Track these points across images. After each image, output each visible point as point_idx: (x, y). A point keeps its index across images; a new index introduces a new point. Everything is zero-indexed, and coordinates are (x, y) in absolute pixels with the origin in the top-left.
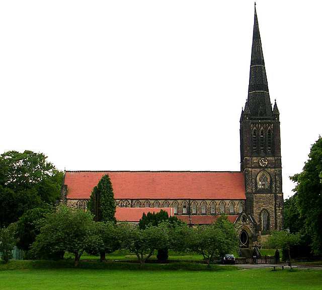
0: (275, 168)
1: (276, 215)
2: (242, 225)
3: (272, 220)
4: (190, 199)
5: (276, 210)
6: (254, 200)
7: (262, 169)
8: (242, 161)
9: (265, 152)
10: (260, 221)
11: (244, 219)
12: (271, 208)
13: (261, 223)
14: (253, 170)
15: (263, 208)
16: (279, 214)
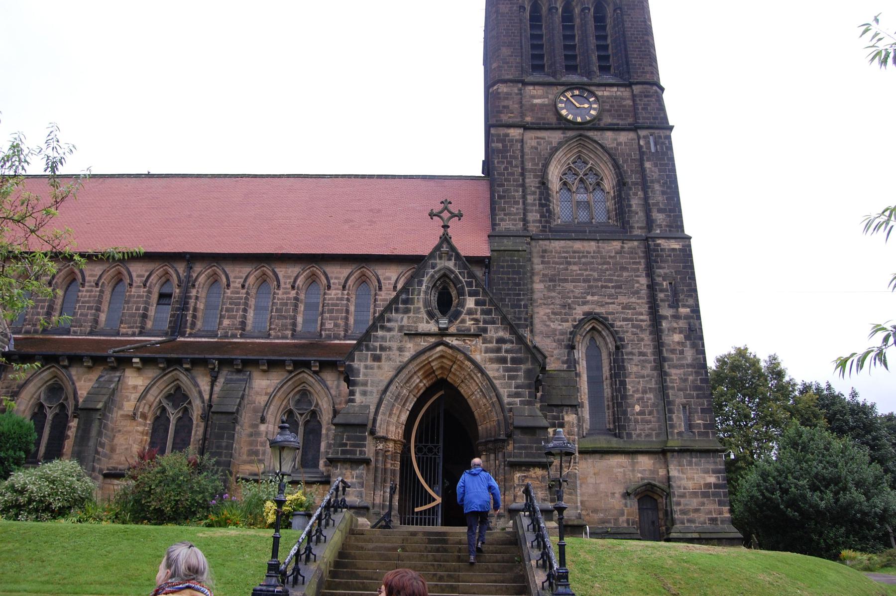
0: (634, 128)
1: (659, 345)
2: (424, 343)
5: (656, 318)
6: (538, 267)
7: (570, 134)
14: (529, 135)
15: (586, 308)
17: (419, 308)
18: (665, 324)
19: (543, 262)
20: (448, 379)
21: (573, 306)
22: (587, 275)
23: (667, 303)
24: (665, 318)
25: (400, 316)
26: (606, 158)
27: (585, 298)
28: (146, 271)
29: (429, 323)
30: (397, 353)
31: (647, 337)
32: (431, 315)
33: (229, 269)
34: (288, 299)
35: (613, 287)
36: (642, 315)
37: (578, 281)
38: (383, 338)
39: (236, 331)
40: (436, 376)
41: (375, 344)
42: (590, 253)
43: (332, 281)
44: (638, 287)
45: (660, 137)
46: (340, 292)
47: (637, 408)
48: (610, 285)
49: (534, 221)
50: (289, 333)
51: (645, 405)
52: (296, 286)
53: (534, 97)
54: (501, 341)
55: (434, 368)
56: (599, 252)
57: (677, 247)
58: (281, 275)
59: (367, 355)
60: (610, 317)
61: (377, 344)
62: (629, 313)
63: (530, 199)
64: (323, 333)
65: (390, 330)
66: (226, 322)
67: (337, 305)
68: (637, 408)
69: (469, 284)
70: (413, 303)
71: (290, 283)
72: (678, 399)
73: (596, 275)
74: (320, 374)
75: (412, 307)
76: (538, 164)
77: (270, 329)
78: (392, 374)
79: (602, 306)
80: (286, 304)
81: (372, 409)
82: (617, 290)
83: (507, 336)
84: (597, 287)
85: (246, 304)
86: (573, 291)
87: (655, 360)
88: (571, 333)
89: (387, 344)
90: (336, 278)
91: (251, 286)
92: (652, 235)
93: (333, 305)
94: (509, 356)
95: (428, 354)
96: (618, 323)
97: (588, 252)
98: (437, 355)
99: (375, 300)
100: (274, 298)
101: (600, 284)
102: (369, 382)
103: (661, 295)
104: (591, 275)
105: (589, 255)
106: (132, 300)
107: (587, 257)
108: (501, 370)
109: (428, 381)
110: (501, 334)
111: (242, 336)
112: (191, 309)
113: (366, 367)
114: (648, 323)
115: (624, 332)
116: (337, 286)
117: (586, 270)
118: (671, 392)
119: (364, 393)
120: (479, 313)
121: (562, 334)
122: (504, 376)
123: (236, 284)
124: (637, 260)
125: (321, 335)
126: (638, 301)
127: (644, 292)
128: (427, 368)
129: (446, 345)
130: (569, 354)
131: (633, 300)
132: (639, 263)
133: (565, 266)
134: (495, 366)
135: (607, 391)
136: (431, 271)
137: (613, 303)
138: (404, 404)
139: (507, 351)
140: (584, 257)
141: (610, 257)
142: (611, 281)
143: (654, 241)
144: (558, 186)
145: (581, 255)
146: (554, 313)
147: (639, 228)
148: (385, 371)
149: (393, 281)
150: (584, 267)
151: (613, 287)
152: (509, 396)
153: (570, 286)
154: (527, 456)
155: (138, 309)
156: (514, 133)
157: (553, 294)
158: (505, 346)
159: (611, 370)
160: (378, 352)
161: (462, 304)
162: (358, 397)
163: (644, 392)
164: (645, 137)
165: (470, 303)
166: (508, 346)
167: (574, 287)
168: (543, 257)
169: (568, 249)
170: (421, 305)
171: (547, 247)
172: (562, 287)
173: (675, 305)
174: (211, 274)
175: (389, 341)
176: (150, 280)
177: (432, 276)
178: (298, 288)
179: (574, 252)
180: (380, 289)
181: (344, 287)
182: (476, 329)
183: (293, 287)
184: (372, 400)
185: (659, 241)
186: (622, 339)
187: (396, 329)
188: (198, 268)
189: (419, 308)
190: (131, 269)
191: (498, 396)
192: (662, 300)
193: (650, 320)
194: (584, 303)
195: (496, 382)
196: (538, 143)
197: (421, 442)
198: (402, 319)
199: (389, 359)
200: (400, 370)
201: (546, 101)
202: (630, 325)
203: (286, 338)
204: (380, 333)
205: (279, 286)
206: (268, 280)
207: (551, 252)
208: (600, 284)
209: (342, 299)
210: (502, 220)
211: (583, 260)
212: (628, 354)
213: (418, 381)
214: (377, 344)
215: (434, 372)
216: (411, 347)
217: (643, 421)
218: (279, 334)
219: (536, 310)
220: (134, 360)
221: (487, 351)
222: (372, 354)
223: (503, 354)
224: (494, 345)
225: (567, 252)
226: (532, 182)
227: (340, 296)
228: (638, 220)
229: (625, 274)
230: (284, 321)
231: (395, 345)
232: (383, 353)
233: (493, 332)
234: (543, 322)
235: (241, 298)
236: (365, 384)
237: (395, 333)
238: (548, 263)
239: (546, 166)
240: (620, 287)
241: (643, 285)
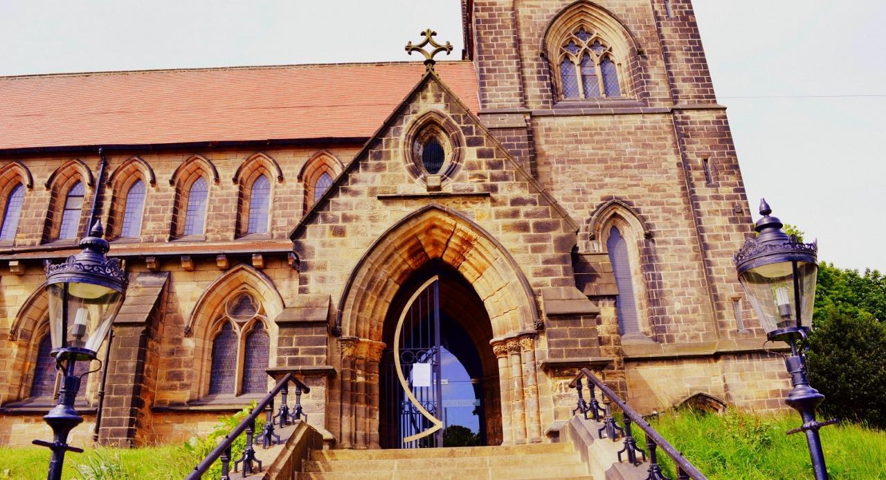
2: (404, 210)
5: (692, 200)
15: (605, 192)
17: (398, 164)
20: (445, 258)
21: (589, 190)
22: (602, 155)
24: (704, 199)
27: (601, 180)
28: (50, 170)
29: (413, 182)
30: (369, 223)
32: (415, 172)
33: (153, 161)
35: (636, 167)
36: (674, 197)
37: (592, 161)
39: (164, 235)
40: (426, 254)
41: (335, 213)
42: (605, 129)
44: (665, 166)
48: (632, 164)
50: (231, 235)
52: (239, 179)
55: (423, 243)
56: (615, 128)
57: (710, 119)
59: (324, 228)
60: (634, 201)
62: (658, 196)
64: (275, 233)
65: (356, 193)
67: (290, 199)
70: (389, 158)
71: (231, 176)
74: (265, 271)
75: (387, 163)
79: (624, 188)
80: (227, 201)
84: (615, 167)
86: (586, 173)
91: (182, 183)
92: (678, 106)
93: (286, 199)
94: (531, 221)
95: (412, 224)
97: (601, 129)
98: (427, 224)
101: (619, 164)
102: (329, 264)
103: (696, 174)
104: (608, 155)
105: (603, 132)
107: (601, 134)
108: (521, 240)
109: (414, 263)
110: (518, 192)
113: (324, 245)
114: (683, 206)
115: (653, 218)
116: (290, 178)
120: (484, 166)
122: (526, 248)
124: (663, 136)
125: (272, 235)
126: (668, 182)
127: (675, 171)
128: (412, 243)
132: (665, 139)
133: (575, 145)
137: (637, 185)
138: (381, 294)
139: (527, 215)
140: (596, 134)
141: (629, 133)
142: (632, 160)
143: (680, 113)
144: (558, 59)
145: (595, 131)
150: (599, 146)
151: (636, 167)
153: (581, 168)
154: (570, 354)
158: (523, 209)
160: (340, 224)
161: (458, 157)
165: (470, 154)
166: (529, 208)
167: (588, 169)
168: (547, 136)
169: (578, 127)
170: (400, 159)
171: (551, 125)
172: (573, 169)
174: (132, 170)
175: (356, 208)
176: (55, 180)
177: (415, 123)
178: (241, 182)
179: (585, 129)
182: (482, 188)
183: (235, 180)
185: (686, 113)
187: (366, 192)
188: (115, 163)
189: (398, 164)
190: (31, 169)
192: (698, 180)
193: (685, 203)
194: (601, 187)
195: (515, 256)
197: (408, 345)
198: (373, 179)
202: (660, 210)
208: (619, 164)
211: (596, 138)
213: (400, 260)
214: (339, 214)
215: (422, 249)
218: (219, 236)
220: (11, 264)
221: (498, 216)
222: (331, 227)
223: (522, 219)
224: (508, 208)
225: (578, 130)
227: (294, 188)
229: (649, 151)
230: (225, 221)
231: (364, 213)
232: (347, 225)
233: (505, 190)
236: (322, 267)
237: (364, 197)
238: (554, 142)
240: (645, 167)
241: (672, 163)
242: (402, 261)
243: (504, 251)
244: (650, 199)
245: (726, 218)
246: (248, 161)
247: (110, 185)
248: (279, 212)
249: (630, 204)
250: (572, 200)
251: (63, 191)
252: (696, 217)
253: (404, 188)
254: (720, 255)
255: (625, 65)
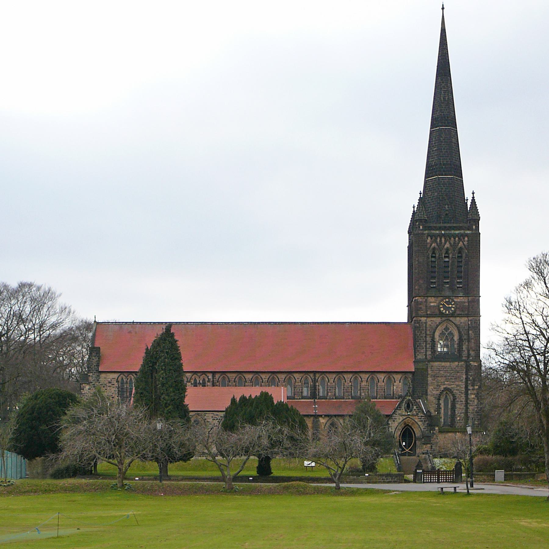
3: (460, 408)
4: (315, 373)
5: (467, 389)
6: (430, 372)
7: (443, 319)
8: (409, 306)
9: (452, 289)
10: (438, 409)
11: (408, 406)
12: (458, 387)
13: (439, 413)
14: (429, 319)
15: (445, 386)
16: (473, 396)
18: (469, 392)
19: (431, 371)
23: (471, 385)
24: (470, 389)
25: (398, 411)
26: (456, 328)
31: (463, 395)
34: (349, 386)
37: (442, 377)
38: (395, 416)
43: (363, 379)
45: (476, 320)
46: (365, 383)
47: (458, 418)
48: (453, 378)
49: (429, 355)
50: (350, 397)
51: (460, 418)
53: (431, 302)
54: (421, 416)
57: (476, 365)
58: (346, 377)
60: (452, 389)
61: (394, 418)
63: (428, 346)
64: (361, 397)
65: (397, 414)
66: (329, 394)
67: (365, 387)
68: (458, 418)
69: (414, 403)
72: (471, 416)
73: (449, 374)
76: (431, 332)
77: (344, 396)
78: (397, 424)
80: (348, 388)
81: (393, 433)
82: (455, 380)
83: (423, 415)
84: (448, 379)
85: (335, 388)
87: (465, 403)
88: (439, 395)
89: (396, 418)
90: (364, 378)
93: (364, 387)
94: (423, 420)
96: (454, 391)
97: (447, 366)
99: (377, 386)
100: (344, 386)
101: (450, 378)
103: (469, 382)
106: (297, 387)
111: (335, 399)
112: (317, 390)
115: (456, 394)
117: (445, 373)
118: (469, 414)
119: (391, 429)
121: (437, 395)
123: (332, 381)
127: (464, 381)
129: (409, 417)
130: (438, 402)
131: (460, 383)
132: (463, 370)
134: (420, 422)
135: (449, 413)
136: (405, 400)
137: (453, 384)
139: (423, 419)
140: (446, 368)
142: (453, 377)
146: (434, 388)
147: (465, 357)
148: (396, 424)
149: (383, 379)
152: (423, 429)
153: (440, 378)
155: (299, 390)
156: (423, 319)
157: (434, 381)
159: (451, 406)
160: (394, 420)
162: (390, 430)
163: (461, 413)
164: (471, 320)
165: (415, 407)
166: (423, 418)
170: (403, 408)
173: (473, 386)
180: (379, 382)
181: (367, 382)
183: (350, 382)
184: (393, 431)
185: (471, 363)
186: (455, 397)
188: (317, 375)
191: (421, 429)
192: (469, 384)
195: (420, 426)
196: (432, 323)
199: (396, 421)
200: (399, 424)
201: (435, 304)
203: (349, 399)
204: (394, 415)
205: (345, 382)
206: (341, 378)
207: (434, 366)
208: (450, 378)
209: (366, 386)
210: (418, 355)
211: (445, 369)
212: (457, 401)
216: (401, 418)
217: (460, 422)
218: (347, 398)
219: (428, 387)
223: (422, 420)
224: (420, 417)
225: (440, 367)
226: (429, 339)
227: (366, 384)
228: (465, 354)
229: (458, 374)
231: (398, 418)
234: (431, 391)
235: (333, 386)
236: (392, 427)
239: (434, 333)
240: (456, 379)
242: (403, 426)
243: (418, 425)
244: (456, 389)
245: (474, 396)
246: (353, 376)
247: (317, 382)
248: (362, 391)
249: (451, 390)
250: (436, 388)
251: (303, 382)
252: (467, 394)
253: (404, 413)
254: (471, 406)
255: (457, 342)
